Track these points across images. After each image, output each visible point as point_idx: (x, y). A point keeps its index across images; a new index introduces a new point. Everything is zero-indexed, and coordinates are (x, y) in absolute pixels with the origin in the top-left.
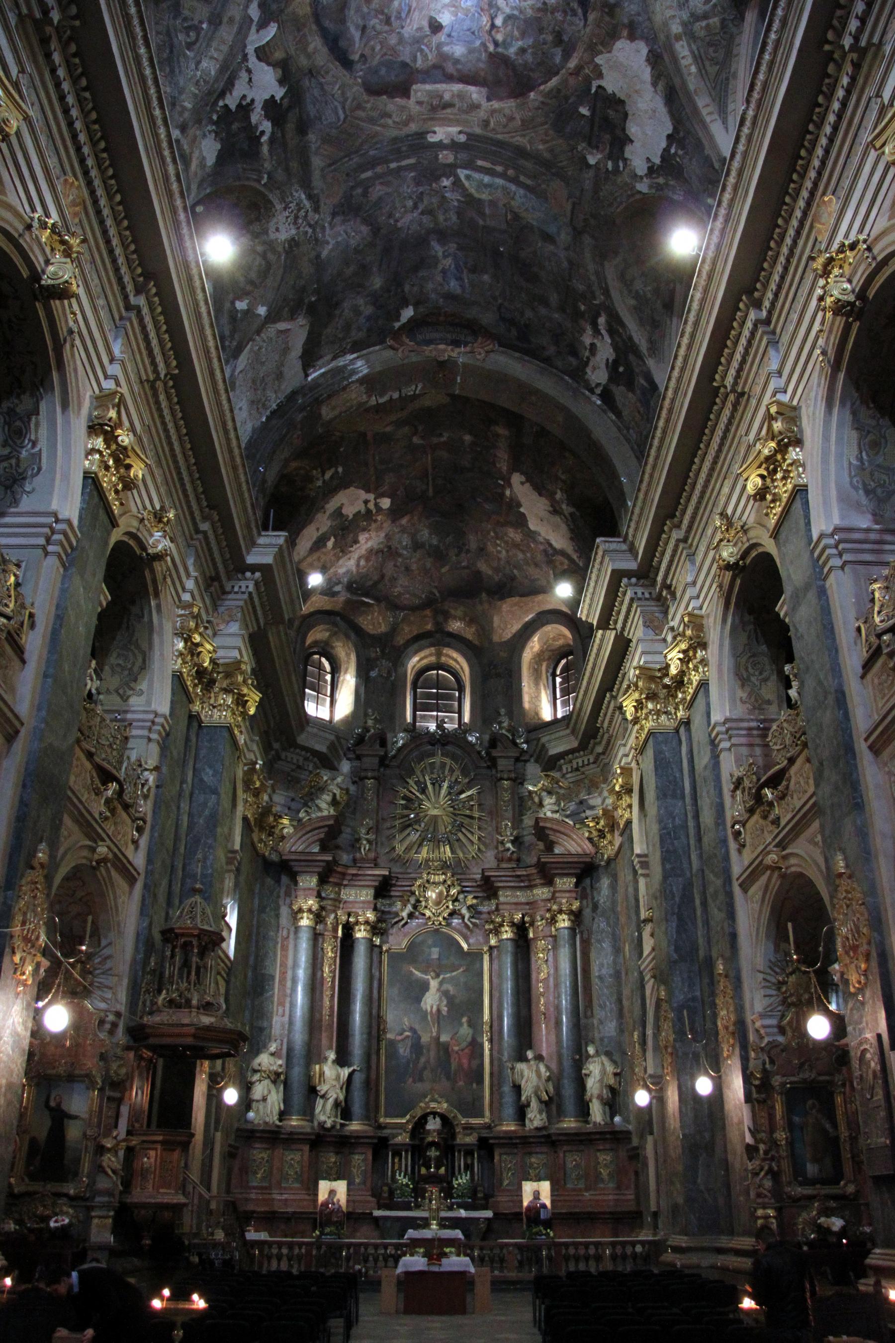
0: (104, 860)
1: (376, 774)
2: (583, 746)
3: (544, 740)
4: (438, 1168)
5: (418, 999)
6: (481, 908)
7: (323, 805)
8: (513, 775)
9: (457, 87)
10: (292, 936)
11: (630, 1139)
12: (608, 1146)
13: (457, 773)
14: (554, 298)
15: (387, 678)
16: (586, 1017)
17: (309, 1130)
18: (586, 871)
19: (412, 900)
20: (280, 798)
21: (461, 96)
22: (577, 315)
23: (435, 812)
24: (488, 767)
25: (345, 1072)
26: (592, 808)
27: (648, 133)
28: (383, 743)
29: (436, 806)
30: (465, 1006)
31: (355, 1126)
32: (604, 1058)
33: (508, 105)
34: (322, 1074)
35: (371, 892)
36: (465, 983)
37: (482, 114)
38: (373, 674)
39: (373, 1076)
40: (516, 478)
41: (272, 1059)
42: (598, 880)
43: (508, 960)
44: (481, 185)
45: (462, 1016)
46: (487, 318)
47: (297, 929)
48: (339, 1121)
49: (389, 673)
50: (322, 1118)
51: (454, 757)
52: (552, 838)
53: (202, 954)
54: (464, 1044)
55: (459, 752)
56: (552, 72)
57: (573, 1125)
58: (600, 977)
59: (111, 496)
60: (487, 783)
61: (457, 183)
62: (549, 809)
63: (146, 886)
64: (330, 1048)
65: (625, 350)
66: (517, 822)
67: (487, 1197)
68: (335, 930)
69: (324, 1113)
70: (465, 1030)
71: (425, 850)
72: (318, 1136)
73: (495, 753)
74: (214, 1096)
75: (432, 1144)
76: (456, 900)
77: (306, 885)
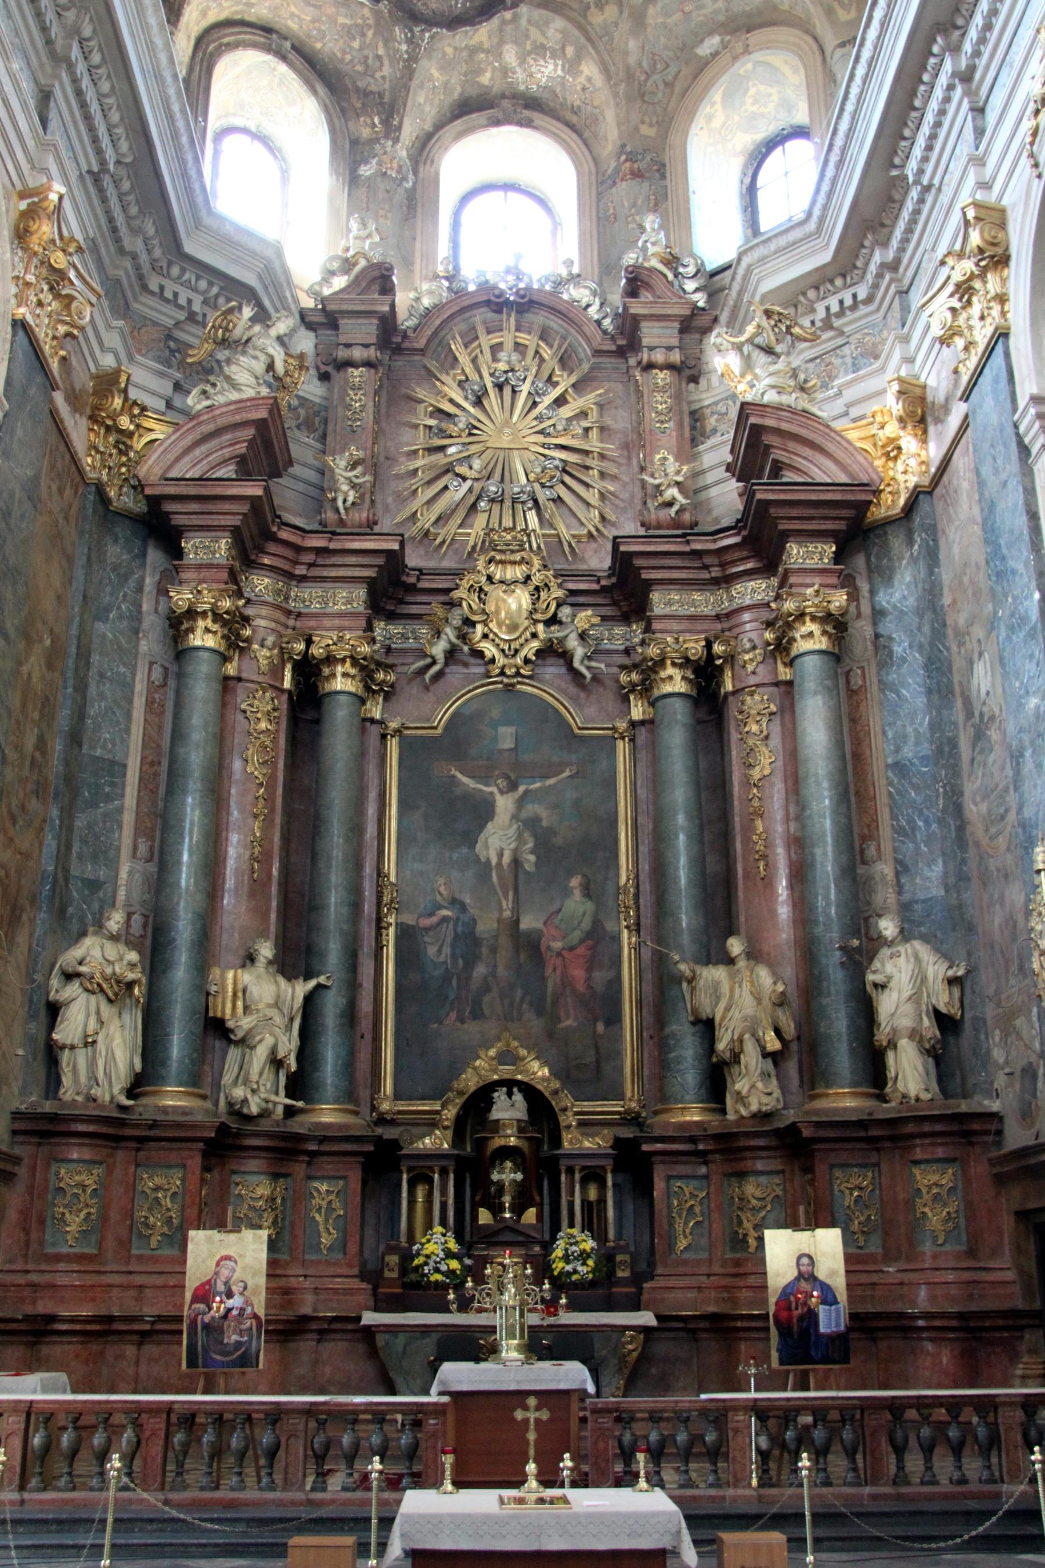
1: (372, 353)
4: (519, 1210)
5: (470, 839)
6: (606, 644)
8: (676, 357)
10: (172, 683)
11: (999, 1133)
12: (940, 1152)
16: (864, 862)
17: (199, 1118)
19: (457, 622)
23: (505, 441)
24: (621, 353)
25: (302, 988)
28: (387, 288)
30: (574, 851)
31: (328, 1114)
32: (917, 944)
35: (361, 593)
36: (577, 803)
39: (365, 1005)
41: (112, 951)
42: (885, 550)
43: (676, 739)
45: (570, 874)
47: (180, 653)
48: (283, 1100)
50: (239, 1093)
51: (544, 335)
52: (777, 454)
54: (576, 935)
55: (555, 324)
57: (849, 1103)
58: (900, 768)
64: (264, 934)
67: (638, 1279)
68: (277, 672)
70: (577, 905)
71: (480, 521)
72: (223, 1129)
73: (637, 308)
75: (506, 1153)
76: (553, 621)
77: (203, 557)
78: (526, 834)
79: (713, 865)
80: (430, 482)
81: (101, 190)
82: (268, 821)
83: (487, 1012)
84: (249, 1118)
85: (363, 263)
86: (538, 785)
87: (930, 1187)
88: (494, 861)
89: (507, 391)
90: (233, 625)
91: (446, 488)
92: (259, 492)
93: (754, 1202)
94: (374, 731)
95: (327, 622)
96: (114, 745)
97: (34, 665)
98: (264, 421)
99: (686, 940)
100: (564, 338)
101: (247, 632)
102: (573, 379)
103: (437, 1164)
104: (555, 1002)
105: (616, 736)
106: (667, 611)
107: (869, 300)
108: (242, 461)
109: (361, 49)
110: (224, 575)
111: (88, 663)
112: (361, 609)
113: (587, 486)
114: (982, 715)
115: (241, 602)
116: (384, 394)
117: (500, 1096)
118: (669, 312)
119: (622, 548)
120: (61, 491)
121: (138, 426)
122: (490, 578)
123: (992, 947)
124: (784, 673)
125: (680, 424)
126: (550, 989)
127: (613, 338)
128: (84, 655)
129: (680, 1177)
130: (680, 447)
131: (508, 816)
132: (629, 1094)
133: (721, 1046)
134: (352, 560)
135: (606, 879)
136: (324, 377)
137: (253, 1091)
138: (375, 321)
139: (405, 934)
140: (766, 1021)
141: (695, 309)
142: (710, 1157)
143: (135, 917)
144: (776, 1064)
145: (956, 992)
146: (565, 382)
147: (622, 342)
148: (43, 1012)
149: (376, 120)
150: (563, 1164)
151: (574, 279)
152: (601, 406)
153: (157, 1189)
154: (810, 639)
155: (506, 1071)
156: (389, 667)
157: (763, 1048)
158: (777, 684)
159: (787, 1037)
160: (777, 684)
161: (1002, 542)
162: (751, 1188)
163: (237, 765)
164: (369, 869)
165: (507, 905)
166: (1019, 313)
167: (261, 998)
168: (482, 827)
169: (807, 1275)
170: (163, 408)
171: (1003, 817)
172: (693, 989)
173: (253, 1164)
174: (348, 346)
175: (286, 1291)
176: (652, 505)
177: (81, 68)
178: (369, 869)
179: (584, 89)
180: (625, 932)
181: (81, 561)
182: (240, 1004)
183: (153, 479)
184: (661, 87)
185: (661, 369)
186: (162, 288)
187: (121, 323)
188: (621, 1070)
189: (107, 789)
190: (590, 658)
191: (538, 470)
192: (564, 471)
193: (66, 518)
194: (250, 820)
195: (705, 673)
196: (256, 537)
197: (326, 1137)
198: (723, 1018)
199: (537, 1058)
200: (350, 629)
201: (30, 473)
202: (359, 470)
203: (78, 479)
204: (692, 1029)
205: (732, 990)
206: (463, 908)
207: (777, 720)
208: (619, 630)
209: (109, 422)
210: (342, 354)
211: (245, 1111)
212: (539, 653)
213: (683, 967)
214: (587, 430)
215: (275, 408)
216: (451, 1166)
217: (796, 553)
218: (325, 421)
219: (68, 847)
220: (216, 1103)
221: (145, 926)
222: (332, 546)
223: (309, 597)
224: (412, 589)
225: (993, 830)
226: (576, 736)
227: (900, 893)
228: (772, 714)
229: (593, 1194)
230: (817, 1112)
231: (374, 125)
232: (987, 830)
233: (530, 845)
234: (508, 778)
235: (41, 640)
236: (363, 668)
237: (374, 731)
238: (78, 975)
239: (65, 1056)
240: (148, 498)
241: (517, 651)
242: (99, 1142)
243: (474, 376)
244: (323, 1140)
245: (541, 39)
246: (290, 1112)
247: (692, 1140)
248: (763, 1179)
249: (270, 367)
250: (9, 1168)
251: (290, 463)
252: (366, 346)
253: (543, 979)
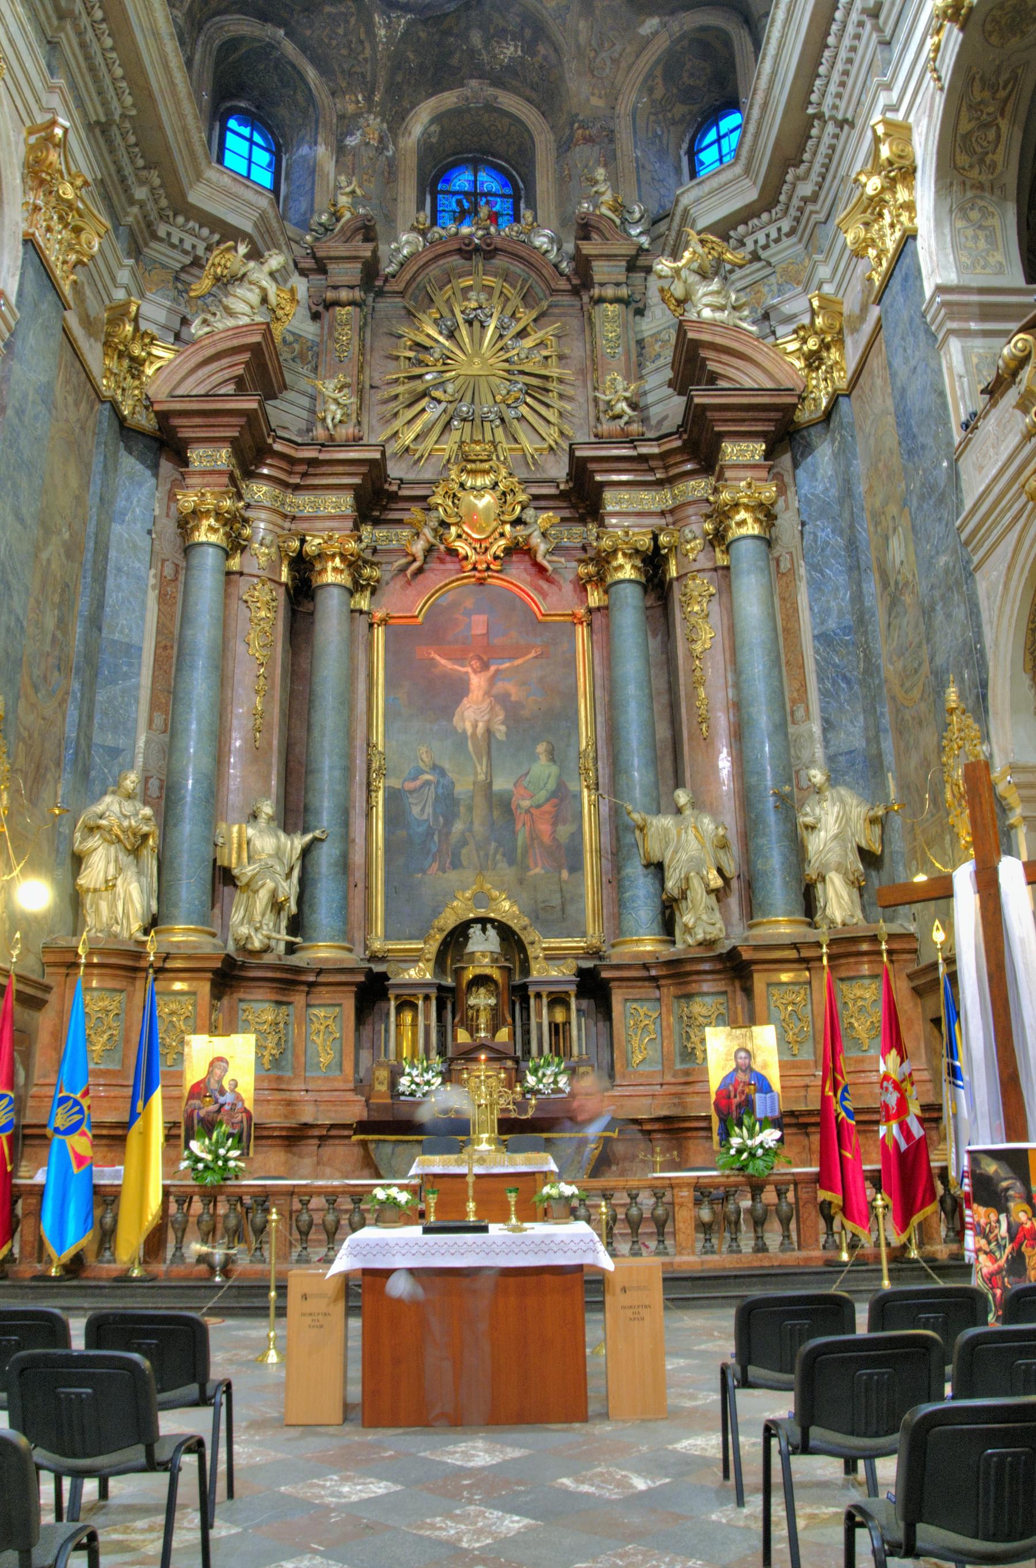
1: (357, 294)
2: (769, 200)
3: (685, 201)
7: (239, 306)
8: (624, 292)
13: (516, 301)
15: (381, 148)
16: (794, 723)
17: (208, 950)
18: (785, 433)
19: (434, 524)
20: (155, 310)
25: (299, 842)
26: (789, 319)
30: (540, 723)
31: (322, 951)
32: (843, 791)
36: (541, 680)
38: (351, 141)
39: (358, 858)
41: (128, 807)
45: (536, 741)
49: (381, 140)
50: (244, 930)
51: (506, 276)
52: (712, 366)
54: (542, 795)
55: (517, 268)
60: (574, 323)
62: (707, 305)
70: (543, 770)
71: (455, 436)
72: (229, 961)
73: (587, 248)
75: (481, 981)
76: (518, 522)
77: (207, 465)
78: (498, 708)
79: (663, 731)
80: (410, 405)
81: (109, 142)
82: (267, 696)
83: (465, 863)
84: (253, 953)
85: (347, 215)
86: (507, 665)
87: (855, 1000)
88: (469, 731)
89: (476, 324)
90: (235, 526)
91: (423, 410)
92: (254, 405)
93: (701, 1019)
94: (362, 621)
95: (319, 524)
96: (130, 630)
97: (52, 552)
98: (259, 343)
99: (637, 793)
100: (525, 281)
101: (247, 532)
102: (534, 314)
103: (421, 992)
104: (525, 853)
105: (575, 620)
106: (617, 508)
107: (792, 232)
108: (240, 382)
109: (345, 35)
110: (225, 480)
111: (106, 558)
112: (349, 512)
113: (547, 406)
114: (897, 583)
115: (241, 504)
116: (368, 330)
117: (475, 931)
118: (617, 252)
119: (578, 453)
120: (77, 404)
121: (149, 354)
122: (462, 485)
123: (908, 788)
124: (722, 560)
125: (627, 353)
126: (520, 842)
127: (569, 279)
128: (102, 550)
129: (635, 1000)
130: (628, 369)
131: (481, 693)
132: (591, 931)
133: (669, 884)
134: (340, 469)
135: (568, 745)
136: (316, 316)
137: (257, 930)
138: (359, 266)
139: (393, 797)
140: (710, 862)
141: (641, 250)
142: (662, 982)
143: (151, 781)
144: (718, 900)
145: (877, 830)
146: (526, 316)
147: (576, 281)
148: (68, 861)
149: (360, 98)
150: (532, 991)
152: (558, 337)
153: (172, 1013)
154: (746, 526)
155: (481, 912)
156: (372, 564)
157: (707, 885)
158: (715, 569)
159: (728, 875)
160: (715, 569)
161: (913, 422)
162: (698, 1007)
163: (241, 648)
164: (360, 742)
165: (481, 770)
166: (924, 221)
167: (263, 848)
168: (458, 702)
169: (746, 1073)
170: (172, 340)
171: (916, 671)
172: (644, 836)
173: (260, 994)
174: (335, 288)
175: (290, 1103)
176: (604, 418)
177: (85, 21)
178: (360, 742)
179: (541, 67)
180: (585, 792)
181: (97, 466)
182: (245, 855)
183: (162, 396)
184: (609, 62)
185: (611, 303)
186: (169, 234)
187: (132, 262)
188: (584, 911)
189: (125, 669)
190: (551, 553)
191: (504, 392)
192: (527, 393)
193: (82, 428)
194: (253, 694)
195: (653, 562)
198: (672, 859)
199: (508, 898)
200: (339, 530)
201: (43, 379)
202: (346, 391)
203: (94, 396)
204: (646, 871)
205: (679, 835)
206: (442, 773)
207: (715, 600)
208: (578, 529)
209: (122, 347)
210: (330, 295)
211: (249, 946)
212: (508, 551)
213: (636, 816)
214: (546, 358)
215: (267, 332)
216: (433, 993)
217: (732, 451)
218: (317, 355)
219: (90, 717)
220: (225, 942)
221: (161, 788)
222: (322, 456)
223: (303, 503)
224: (394, 497)
225: (908, 684)
226: (540, 622)
227: (826, 747)
228: (712, 595)
229: (559, 1017)
230: (754, 937)
231: (358, 102)
232: (902, 685)
233: (501, 717)
234: (480, 658)
235: (59, 533)
236: (350, 565)
237: (362, 621)
238: (99, 827)
239: (88, 900)
240: (157, 414)
241: (487, 549)
242: (118, 972)
243: (446, 313)
244: (320, 972)
245: (501, 23)
246: (291, 949)
247: (646, 967)
248: (708, 1000)
249: (264, 300)
250: (39, 994)
251: (285, 387)
252: (352, 287)
253: (514, 833)
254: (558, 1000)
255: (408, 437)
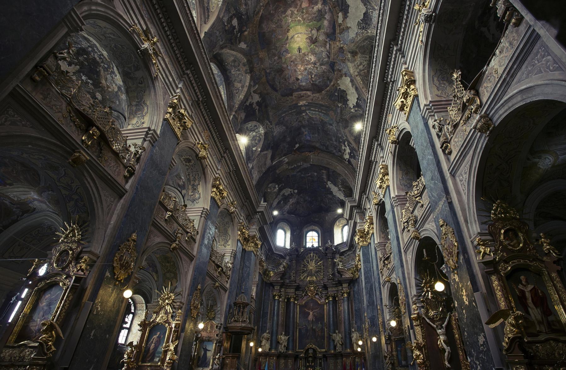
0: (218, 287)
9: (304, 92)
14: (334, 139)
21: (305, 94)
22: (340, 142)
27: (352, 99)
29: (312, 266)
31: (290, 352)
33: (317, 95)
34: (281, 338)
37: (311, 98)
40: (329, 183)
44: (312, 114)
46: (318, 145)
47: (275, 300)
51: (316, 254)
53: (244, 308)
56: (327, 86)
59: (218, 201)
61: (307, 114)
63: (230, 292)
65: (352, 149)
66: (333, 269)
69: (281, 349)
74: (248, 344)
75: (310, 356)
139: (300, 329)
151: (319, 246)
167: (283, 338)
196: (282, 285)
197: (290, 354)
223: (288, 290)
254: (320, 359)
255: (302, 278)
